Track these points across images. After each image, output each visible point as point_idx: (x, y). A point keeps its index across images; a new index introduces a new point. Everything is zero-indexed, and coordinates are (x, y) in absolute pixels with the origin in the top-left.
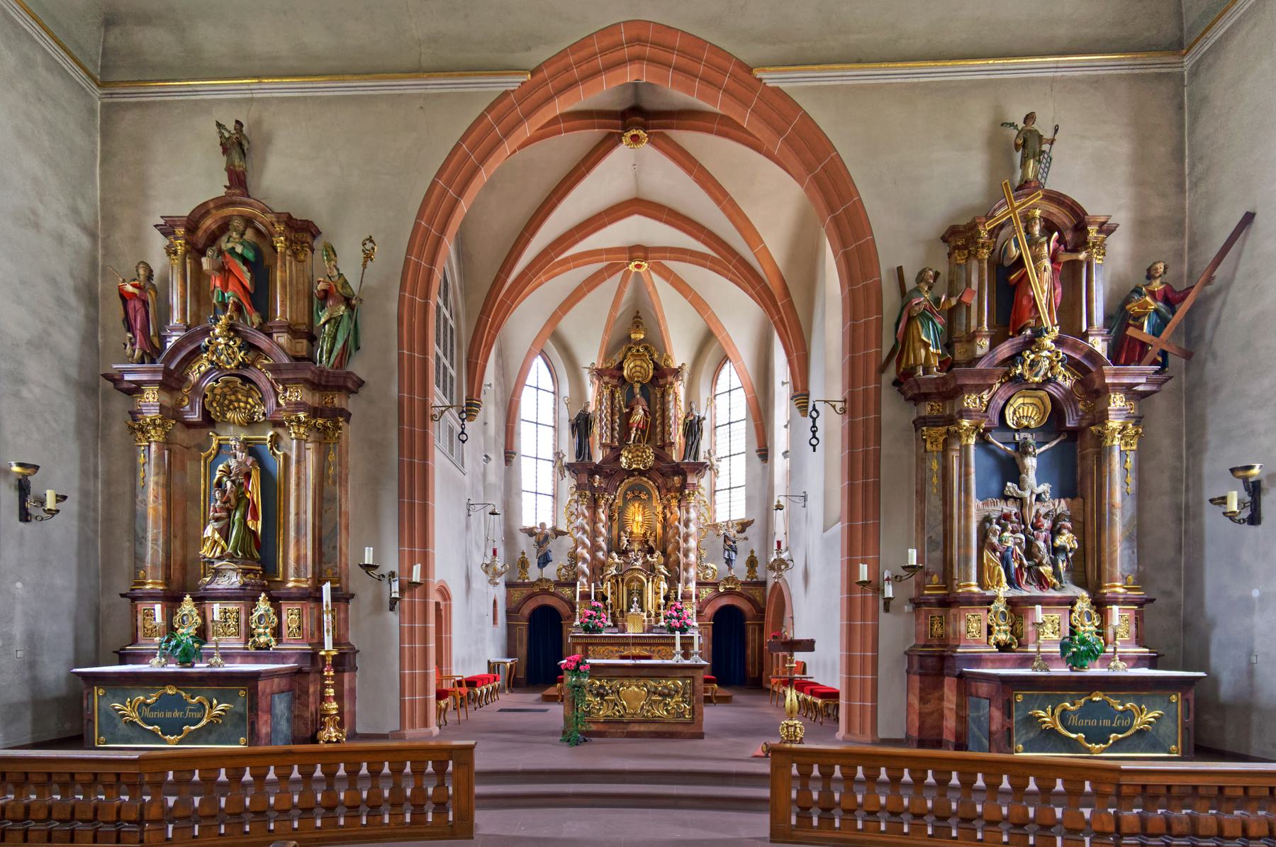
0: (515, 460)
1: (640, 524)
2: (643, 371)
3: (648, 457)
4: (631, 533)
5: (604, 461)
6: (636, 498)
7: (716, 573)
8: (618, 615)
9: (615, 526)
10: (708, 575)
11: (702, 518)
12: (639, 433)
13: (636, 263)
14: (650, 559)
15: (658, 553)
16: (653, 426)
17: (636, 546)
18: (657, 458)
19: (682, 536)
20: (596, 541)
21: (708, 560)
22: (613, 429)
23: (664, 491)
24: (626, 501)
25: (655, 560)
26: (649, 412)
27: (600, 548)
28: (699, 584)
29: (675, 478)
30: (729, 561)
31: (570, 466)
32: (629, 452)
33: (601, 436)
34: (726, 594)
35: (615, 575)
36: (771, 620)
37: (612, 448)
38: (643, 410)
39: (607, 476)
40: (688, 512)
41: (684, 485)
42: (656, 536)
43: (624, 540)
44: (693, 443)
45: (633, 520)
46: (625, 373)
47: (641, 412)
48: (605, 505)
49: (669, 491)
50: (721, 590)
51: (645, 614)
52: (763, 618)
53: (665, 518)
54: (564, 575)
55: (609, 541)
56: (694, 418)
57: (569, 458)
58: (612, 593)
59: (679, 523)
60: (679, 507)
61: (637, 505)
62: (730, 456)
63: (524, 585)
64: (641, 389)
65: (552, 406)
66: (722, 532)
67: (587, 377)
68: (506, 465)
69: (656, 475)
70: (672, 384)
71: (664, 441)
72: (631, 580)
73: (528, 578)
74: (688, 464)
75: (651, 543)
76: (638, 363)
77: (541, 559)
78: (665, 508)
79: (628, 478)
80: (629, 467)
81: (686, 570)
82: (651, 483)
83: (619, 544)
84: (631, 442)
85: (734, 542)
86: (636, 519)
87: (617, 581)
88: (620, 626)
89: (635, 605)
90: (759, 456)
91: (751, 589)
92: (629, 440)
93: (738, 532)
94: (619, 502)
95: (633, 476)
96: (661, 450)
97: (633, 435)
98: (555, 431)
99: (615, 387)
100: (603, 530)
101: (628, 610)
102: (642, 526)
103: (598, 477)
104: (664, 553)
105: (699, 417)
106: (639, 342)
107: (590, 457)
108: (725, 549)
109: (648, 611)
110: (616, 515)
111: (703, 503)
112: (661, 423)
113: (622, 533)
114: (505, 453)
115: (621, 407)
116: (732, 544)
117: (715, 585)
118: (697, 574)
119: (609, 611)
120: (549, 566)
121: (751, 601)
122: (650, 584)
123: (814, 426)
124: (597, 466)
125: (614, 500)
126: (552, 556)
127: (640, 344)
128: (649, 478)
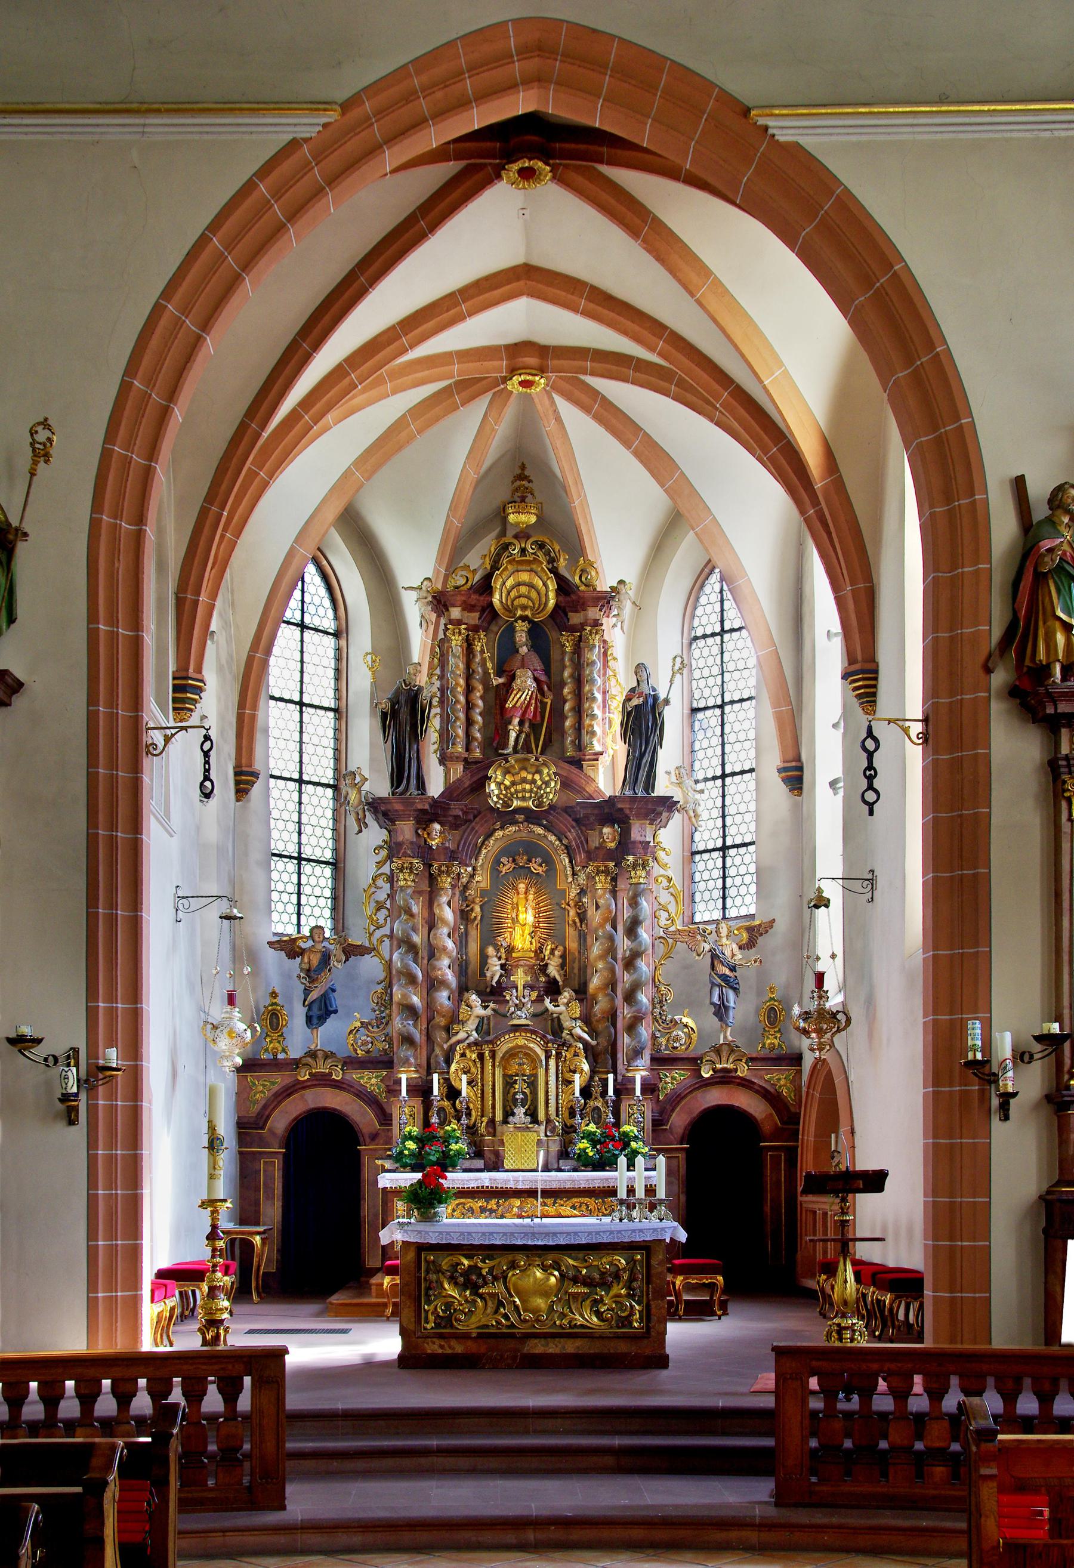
0: (256, 790)
1: (528, 930)
2: (534, 594)
3: (547, 784)
4: (510, 949)
5: (450, 792)
6: (520, 871)
7: (694, 1036)
8: (482, 1129)
9: (475, 935)
10: (676, 1040)
11: (664, 915)
12: (526, 728)
13: (523, 378)
14: (550, 1007)
15: (566, 995)
16: (558, 714)
17: (520, 978)
18: (567, 784)
19: (620, 956)
20: (434, 968)
21: (678, 1007)
22: (469, 722)
23: (581, 857)
24: (500, 882)
25: (562, 1008)
26: (549, 682)
27: (443, 983)
28: (660, 1061)
29: (606, 830)
30: (721, 1011)
31: (375, 806)
32: (504, 775)
33: (445, 737)
34: (717, 1083)
35: (476, 1043)
36: (812, 1139)
37: (467, 762)
38: (536, 679)
39: (454, 824)
40: (634, 903)
41: (625, 845)
42: (563, 957)
43: (494, 968)
44: (642, 755)
45: (516, 921)
46: (496, 600)
47: (530, 683)
48: (453, 887)
49: (590, 856)
50: (706, 1074)
51: (543, 1128)
52: (794, 1135)
53: (582, 917)
54: (365, 1043)
55: (462, 967)
56: (646, 702)
57: (380, 786)
58: (469, 1083)
59: (614, 927)
60: (614, 893)
61: (522, 887)
62: (724, 776)
63: (275, 1065)
64: (531, 633)
65: (333, 664)
66: (707, 947)
67: (413, 609)
68: (238, 800)
69: (565, 822)
70: (597, 624)
71: (579, 747)
72: (511, 1054)
73: (284, 1051)
74: (633, 799)
75: (553, 971)
76: (524, 577)
77: (315, 1008)
78: (582, 892)
79: (502, 828)
80: (506, 805)
81: (631, 1028)
82: (552, 838)
83: (483, 975)
84: (510, 750)
85: (733, 969)
86: (522, 917)
87: (481, 1056)
88: (487, 1155)
89: (520, 1111)
90: (786, 780)
91: (769, 1072)
92: (505, 745)
93: (740, 948)
94: (482, 880)
95: (514, 822)
96: (574, 770)
97: (513, 735)
98: (338, 719)
99: (475, 629)
100: (450, 944)
101: (505, 1122)
102: (532, 934)
103: (437, 827)
104: (581, 992)
105: (655, 698)
106: (523, 534)
107: (421, 785)
108: (713, 984)
109: (548, 1121)
110: (477, 909)
111: (665, 883)
112: (573, 709)
113: (491, 951)
114: (236, 774)
115: (486, 673)
116: (727, 972)
117: (695, 1062)
118: (654, 1037)
119: (464, 1121)
120: (331, 1023)
121: (771, 1097)
122: (552, 1062)
123: (870, 766)
124: (435, 803)
125: (472, 876)
126: (338, 1000)
127: (528, 537)
128: (547, 828)
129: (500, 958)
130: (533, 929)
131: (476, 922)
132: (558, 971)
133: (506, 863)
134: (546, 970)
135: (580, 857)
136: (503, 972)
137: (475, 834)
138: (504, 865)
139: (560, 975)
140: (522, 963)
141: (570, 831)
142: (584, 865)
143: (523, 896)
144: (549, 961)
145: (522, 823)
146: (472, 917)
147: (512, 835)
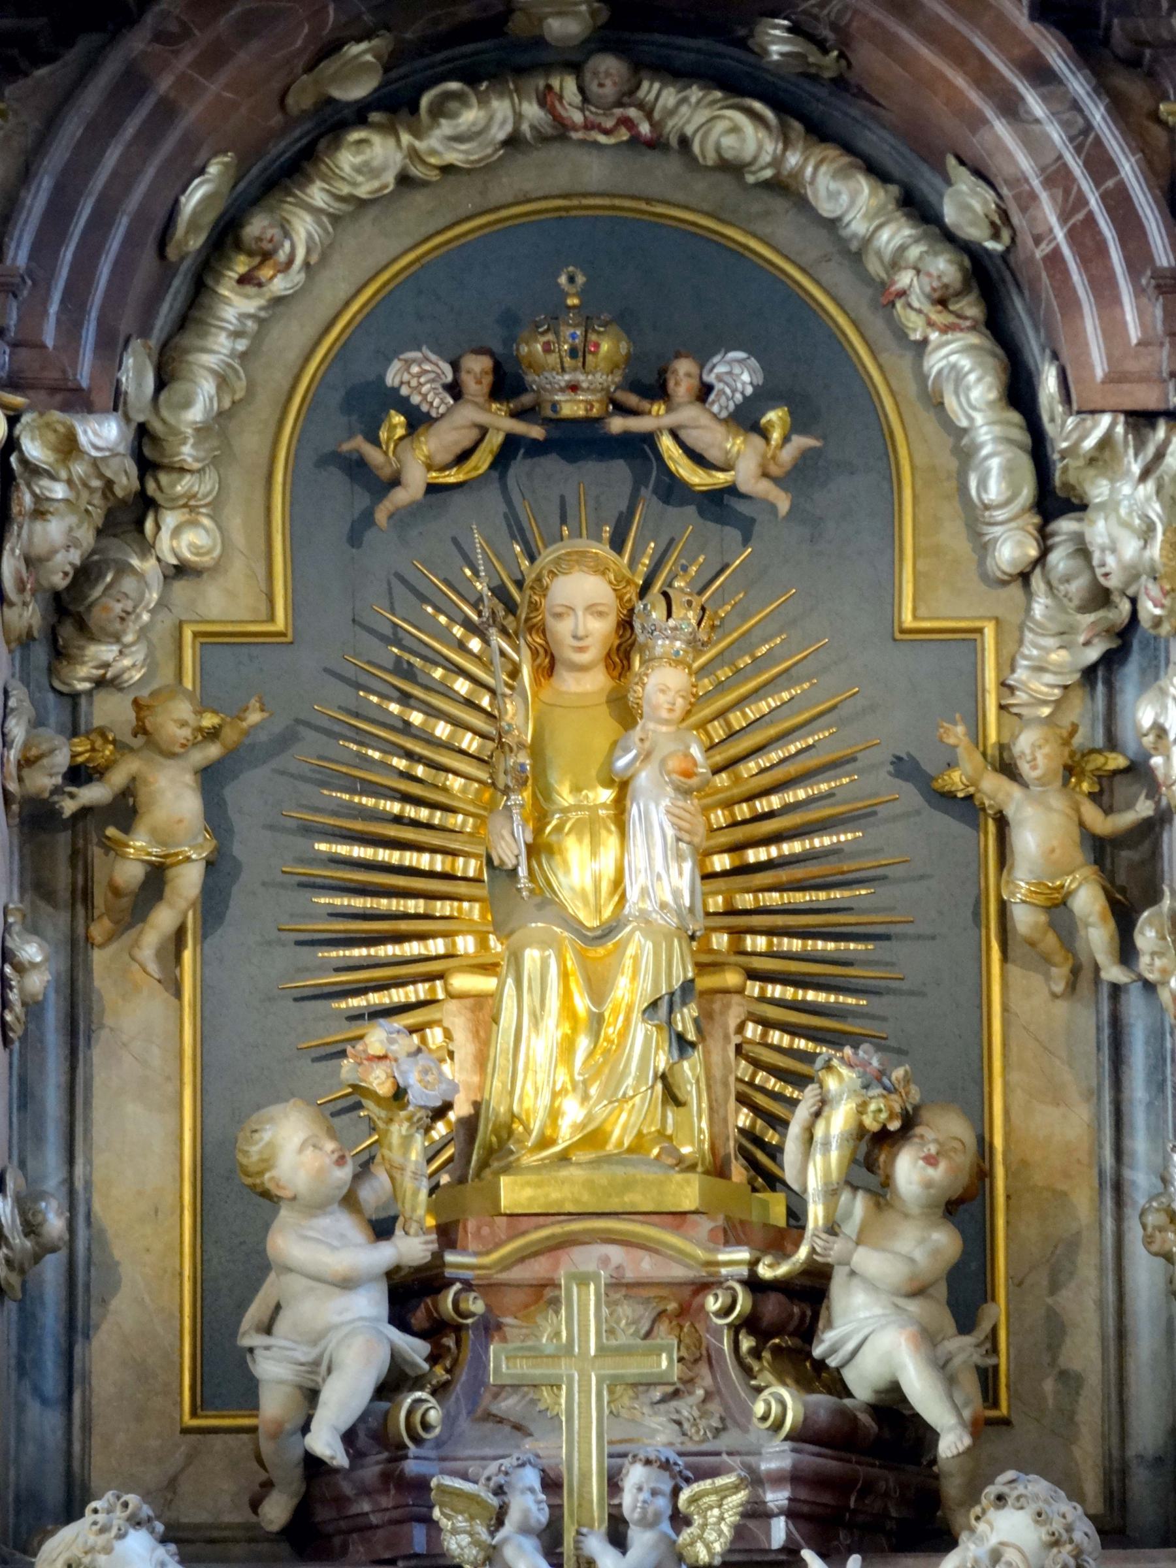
129: (382, 1229)
130: (682, 971)
131: (163, 919)
132: (928, 1338)
133: (436, 401)
134: (808, 1332)
135: (1113, 329)
136: (415, 1349)
137: (150, 136)
138: (418, 421)
139: (943, 1369)
140: (586, 1258)
141: (1011, 107)
142: (1147, 398)
143: (596, 682)
144: (837, 1249)
145: (575, 67)
146: (130, 873)
147: (484, 170)
